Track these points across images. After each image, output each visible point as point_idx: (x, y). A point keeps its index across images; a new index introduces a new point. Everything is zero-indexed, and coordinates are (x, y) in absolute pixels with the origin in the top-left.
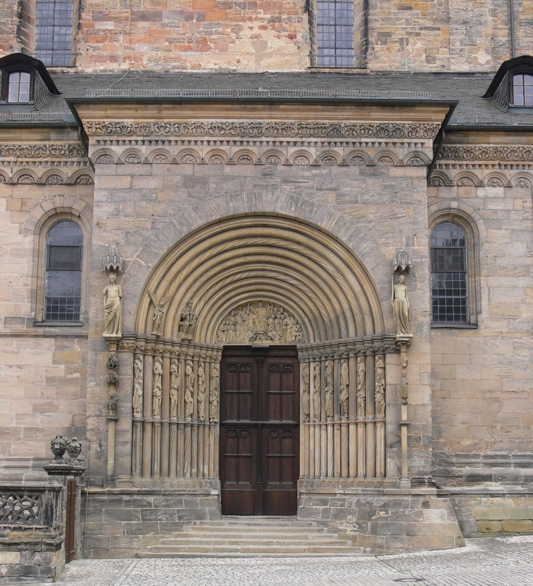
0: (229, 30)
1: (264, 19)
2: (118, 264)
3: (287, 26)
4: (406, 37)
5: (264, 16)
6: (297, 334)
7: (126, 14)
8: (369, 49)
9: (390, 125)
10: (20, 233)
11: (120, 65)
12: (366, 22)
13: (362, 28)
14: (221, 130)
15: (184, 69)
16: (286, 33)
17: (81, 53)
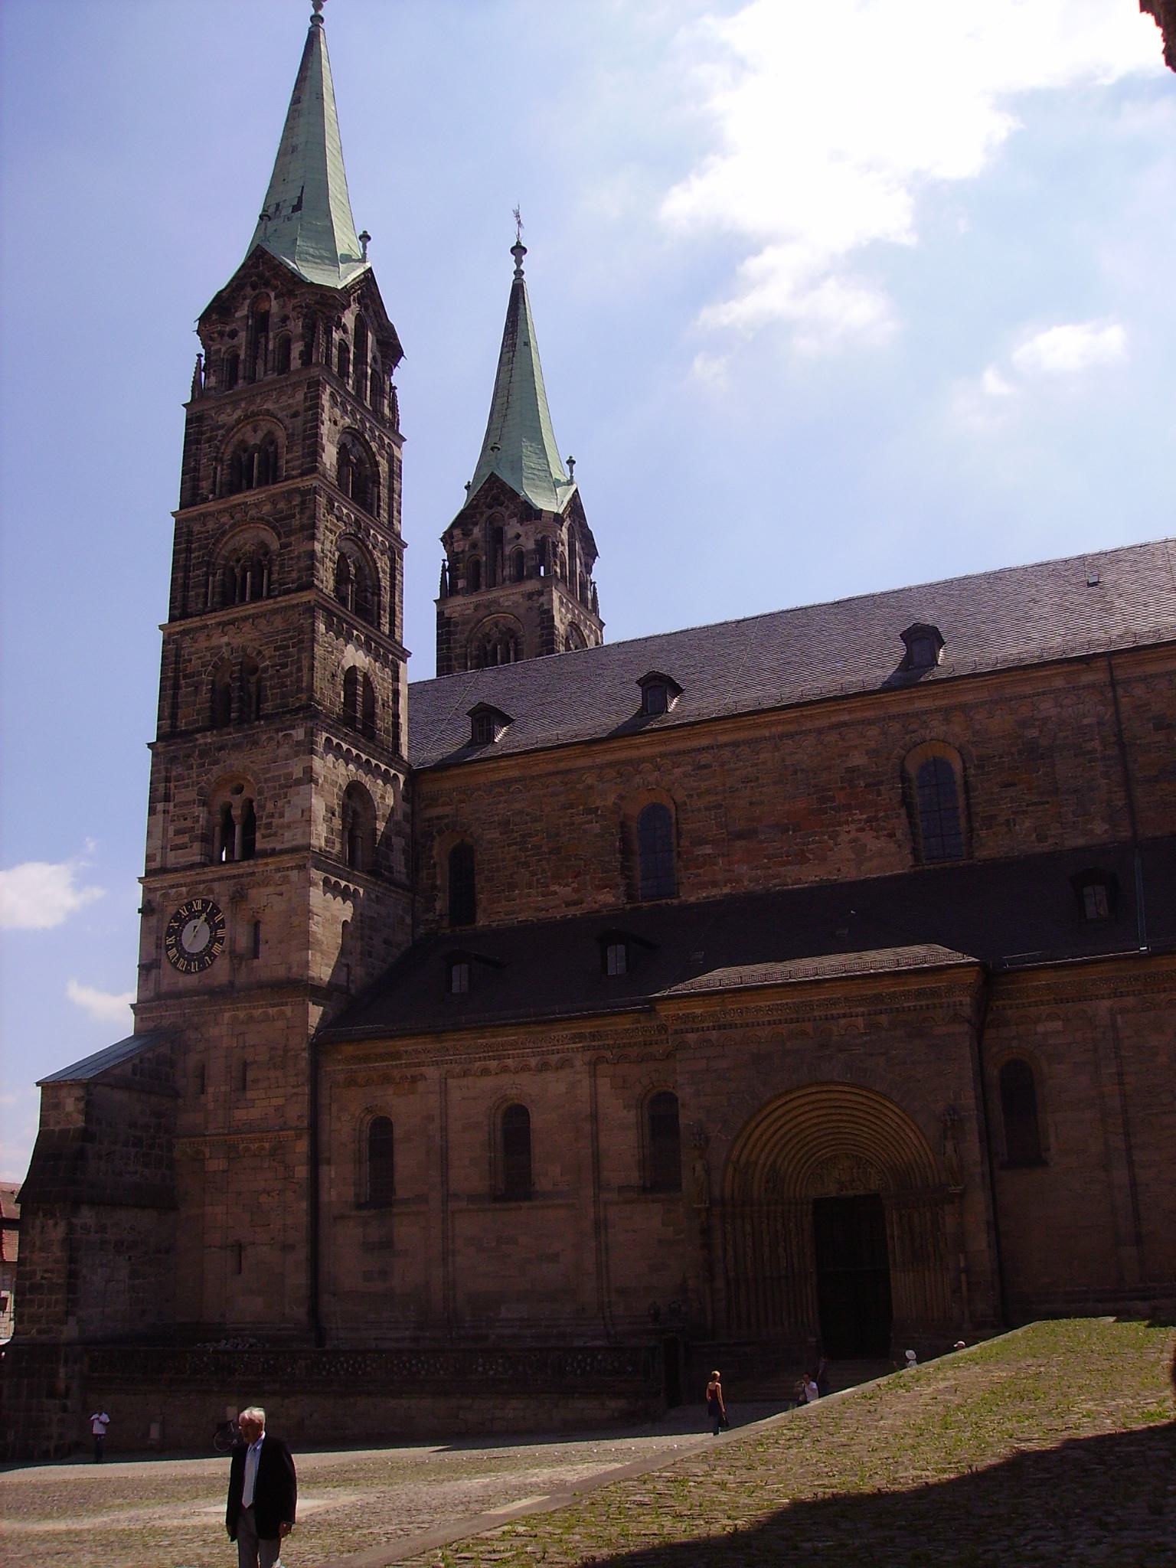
0: (826, 837)
1: (860, 820)
2: (701, 1142)
3: (885, 824)
4: (1012, 817)
5: (861, 817)
6: (880, 1182)
7: (723, 836)
8: (974, 836)
9: (927, 990)
10: (625, 1108)
11: (721, 890)
12: (968, 806)
13: (966, 813)
14: (777, 1012)
15: (785, 885)
16: (886, 832)
17: (683, 883)
